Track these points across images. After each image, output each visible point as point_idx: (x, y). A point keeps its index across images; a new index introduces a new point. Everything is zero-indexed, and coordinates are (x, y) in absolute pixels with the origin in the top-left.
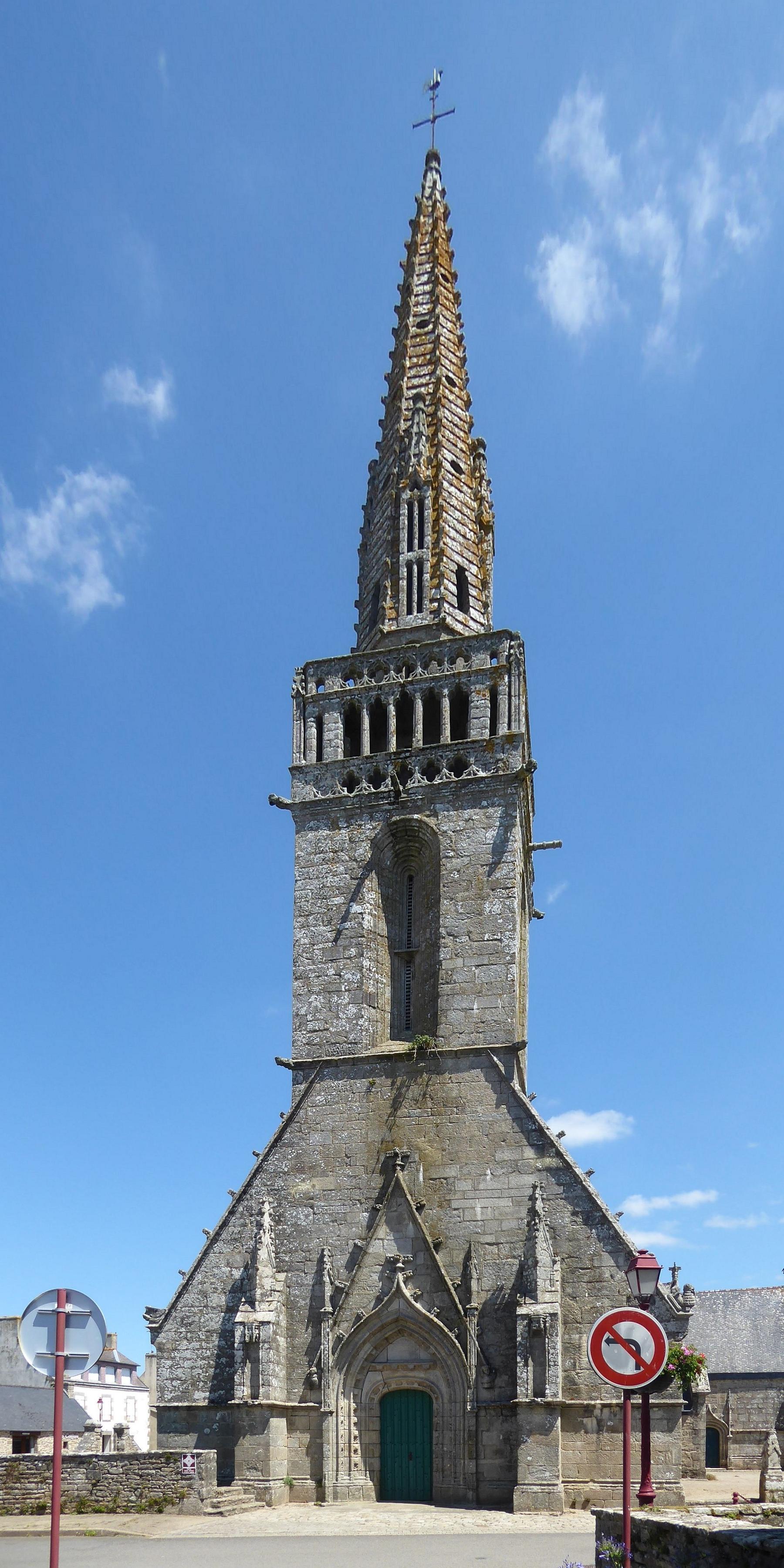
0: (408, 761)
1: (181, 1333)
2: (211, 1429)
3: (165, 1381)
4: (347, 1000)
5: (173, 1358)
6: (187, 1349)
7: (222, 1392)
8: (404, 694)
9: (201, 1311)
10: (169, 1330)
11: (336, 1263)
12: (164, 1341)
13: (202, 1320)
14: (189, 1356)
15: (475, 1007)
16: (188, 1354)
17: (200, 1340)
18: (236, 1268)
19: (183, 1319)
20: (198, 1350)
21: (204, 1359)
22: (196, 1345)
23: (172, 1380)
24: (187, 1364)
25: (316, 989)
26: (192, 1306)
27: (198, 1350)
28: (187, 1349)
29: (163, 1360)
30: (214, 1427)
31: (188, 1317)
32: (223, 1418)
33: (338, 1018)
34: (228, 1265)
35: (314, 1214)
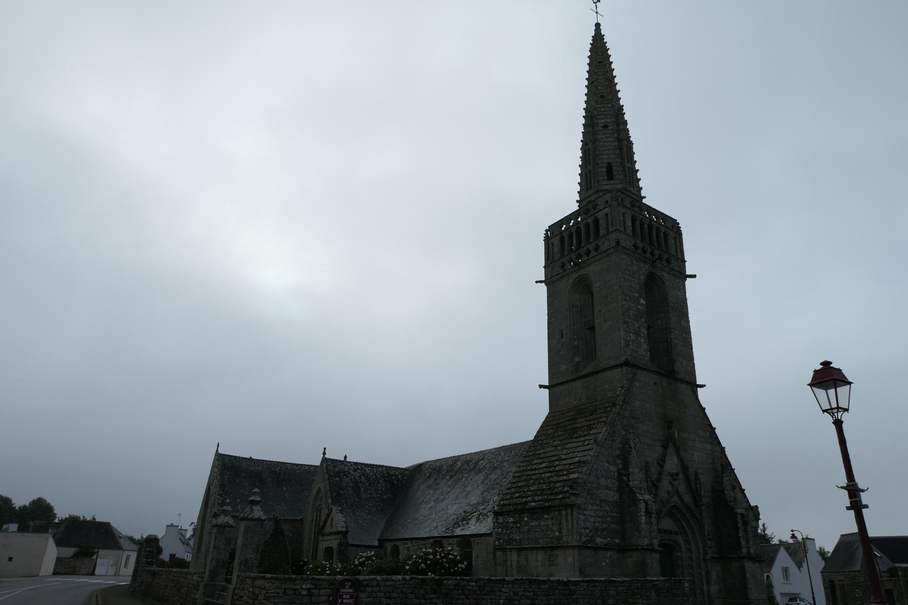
0: (655, 250)
1: (588, 499)
2: (606, 563)
3: (582, 530)
4: (643, 341)
5: (585, 515)
6: (591, 510)
7: (609, 539)
8: (650, 222)
9: (596, 487)
10: (582, 496)
11: (654, 470)
12: (580, 503)
13: (598, 493)
14: (593, 515)
15: (684, 363)
16: (592, 513)
17: (597, 505)
18: (611, 465)
19: (588, 490)
20: (597, 511)
21: (600, 517)
22: (595, 508)
23: (585, 528)
24: (592, 519)
25: (633, 331)
26: (592, 483)
27: (597, 511)
28: (591, 510)
29: (580, 516)
30: (607, 562)
31: (591, 490)
32: (611, 556)
33: (641, 348)
34: (607, 462)
35: (640, 442)
